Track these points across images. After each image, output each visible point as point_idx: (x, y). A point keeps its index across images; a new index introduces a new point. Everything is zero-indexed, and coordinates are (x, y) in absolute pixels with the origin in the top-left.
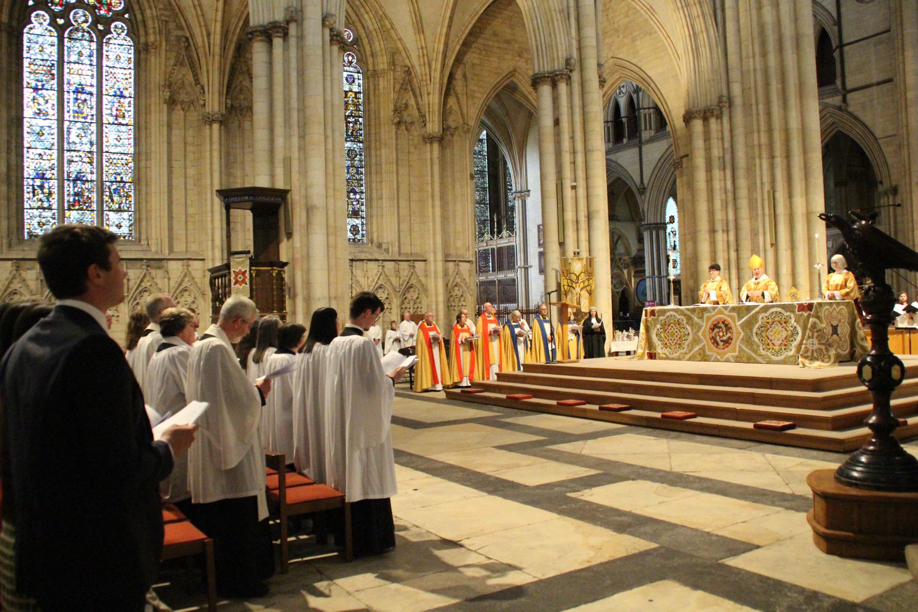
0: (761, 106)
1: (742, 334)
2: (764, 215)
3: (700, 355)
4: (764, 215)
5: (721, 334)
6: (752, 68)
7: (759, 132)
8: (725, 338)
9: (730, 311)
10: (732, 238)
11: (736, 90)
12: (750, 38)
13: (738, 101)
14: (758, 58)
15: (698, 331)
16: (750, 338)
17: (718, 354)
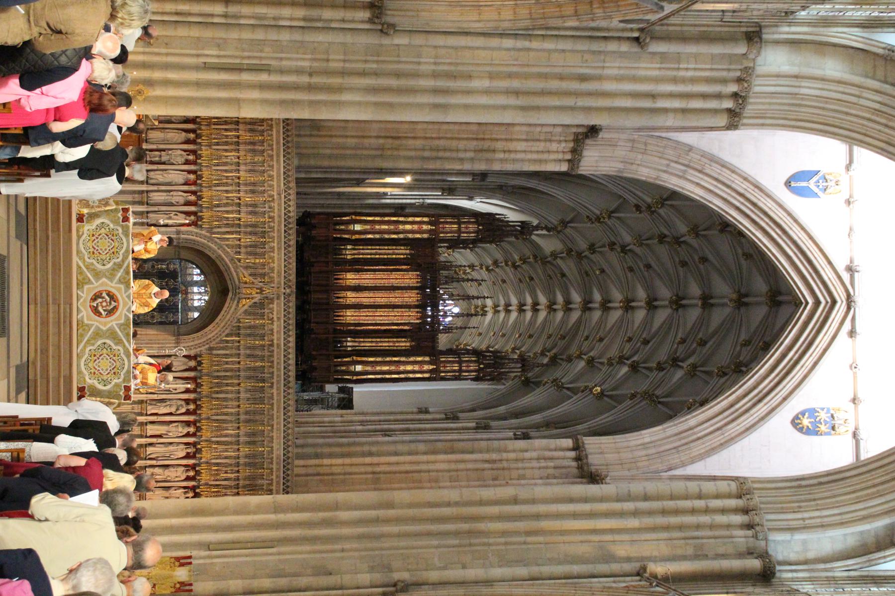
0: (374, 66)
1: (104, 329)
2: (243, 58)
3: (84, 279)
4: (243, 58)
5: (104, 304)
6: (422, 60)
7: (344, 61)
8: (100, 300)
9: (125, 315)
10: (216, 20)
11: (401, 40)
12: (459, 61)
13: (386, 41)
14: (433, 67)
15: (106, 277)
16: (101, 336)
17: (85, 301)
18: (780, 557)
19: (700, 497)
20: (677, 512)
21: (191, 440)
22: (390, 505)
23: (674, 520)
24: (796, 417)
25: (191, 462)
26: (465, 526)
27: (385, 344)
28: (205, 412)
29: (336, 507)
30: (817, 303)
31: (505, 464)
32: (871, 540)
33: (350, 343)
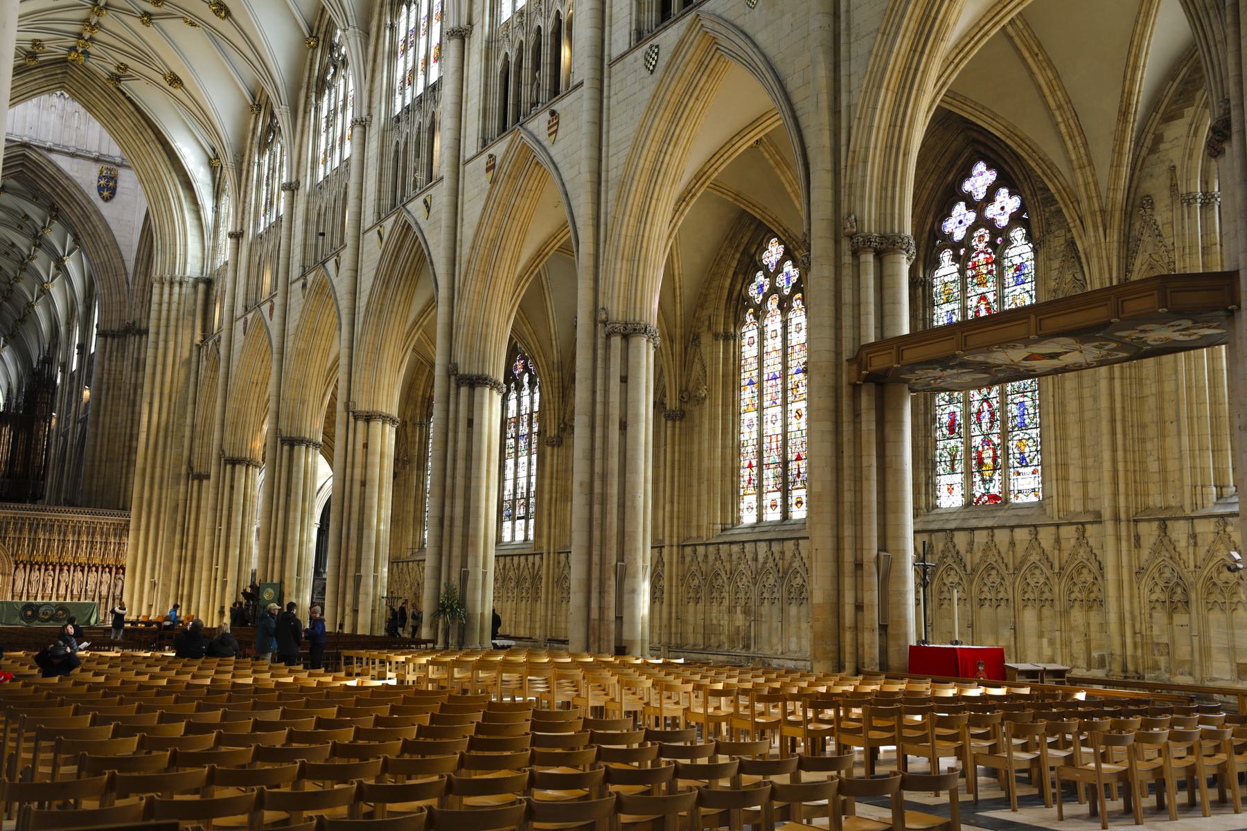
18: (199, 271)
19: (160, 304)
20: (168, 319)
21: (72, 568)
22: (144, 470)
23: (173, 322)
24: (103, 198)
25: (86, 569)
26: (162, 433)
27: (21, 447)
28: (55, 559)
29: (141, 498)
30: (22, 165)
31: (111, 381)
32: (195, 222)
33: (18, 469)
